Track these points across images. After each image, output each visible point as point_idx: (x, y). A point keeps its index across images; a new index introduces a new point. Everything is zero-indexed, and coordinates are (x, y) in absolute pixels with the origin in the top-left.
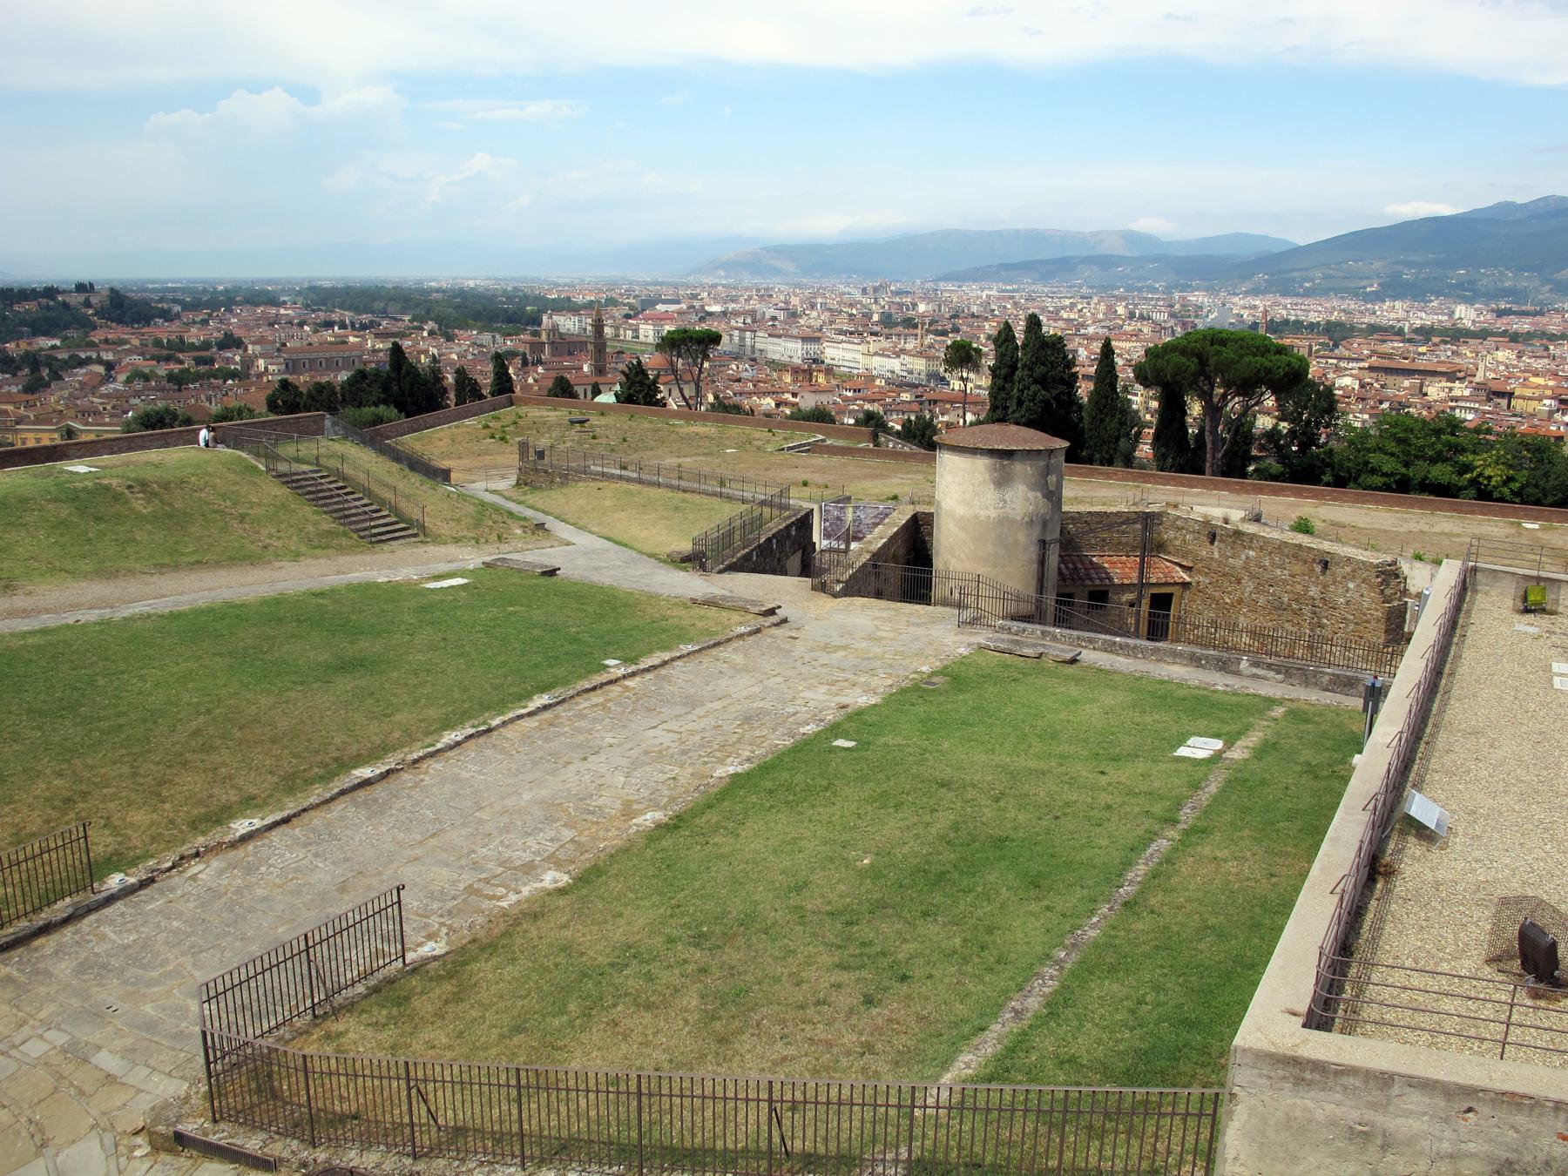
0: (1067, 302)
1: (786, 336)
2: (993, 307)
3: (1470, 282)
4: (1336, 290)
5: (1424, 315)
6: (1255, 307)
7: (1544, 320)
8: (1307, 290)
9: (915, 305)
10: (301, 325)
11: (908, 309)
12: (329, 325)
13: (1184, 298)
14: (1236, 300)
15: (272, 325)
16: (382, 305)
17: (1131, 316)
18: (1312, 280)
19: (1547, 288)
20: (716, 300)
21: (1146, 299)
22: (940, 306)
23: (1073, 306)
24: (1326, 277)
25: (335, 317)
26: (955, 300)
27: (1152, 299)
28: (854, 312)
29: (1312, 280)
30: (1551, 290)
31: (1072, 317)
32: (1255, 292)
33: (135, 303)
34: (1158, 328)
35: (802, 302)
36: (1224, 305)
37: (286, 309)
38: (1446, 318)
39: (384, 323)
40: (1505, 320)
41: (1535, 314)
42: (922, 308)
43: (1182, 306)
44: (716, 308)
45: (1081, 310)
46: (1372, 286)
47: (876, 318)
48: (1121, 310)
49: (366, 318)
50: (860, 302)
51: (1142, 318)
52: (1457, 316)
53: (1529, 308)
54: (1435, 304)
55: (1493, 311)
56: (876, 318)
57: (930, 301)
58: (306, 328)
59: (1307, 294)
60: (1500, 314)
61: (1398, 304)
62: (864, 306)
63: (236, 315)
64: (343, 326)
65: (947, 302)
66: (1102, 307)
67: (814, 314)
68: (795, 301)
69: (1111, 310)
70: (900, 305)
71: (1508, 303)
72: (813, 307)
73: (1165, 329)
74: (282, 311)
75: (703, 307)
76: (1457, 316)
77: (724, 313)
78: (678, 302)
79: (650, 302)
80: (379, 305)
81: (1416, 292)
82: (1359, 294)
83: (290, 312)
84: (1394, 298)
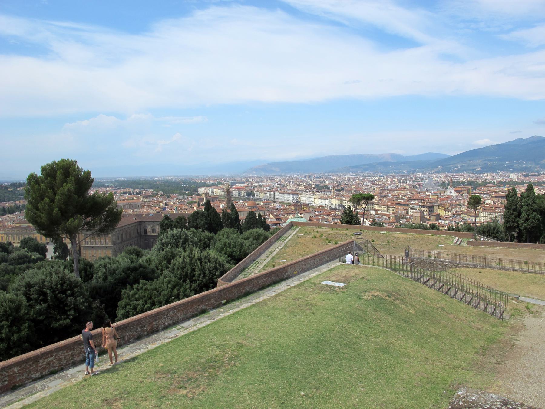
0: (377, 178)
2: (352, 181)
3: (511, 166)
4: (466, 170)
5: (499, 178)
6: (440, 177)
7: (541, 177)
8: (456, 170)
9: (324, 181)
12: (125, 193)
13: (415, 175)
14: (433, 175)
16: (142, 186)
17: (400, 182)
18: (457, 167)
19: (538, 166)
21: (402, 176)
22: (333, 181)
23: (379, 179)
24: (462, 166)
25: (127, 190)
26: (338, 179)
27: (404, 176)
28: (305, 184)
29: (457, 167)
30: (539, 167)
31: (380, 183)
32: (438, 172)
34: (411, 186)
35: (285, 181)
36: (429, 177)
37: (109, 188)
38: (507, 178)
39: (144, 192)
40: (527, 178)
41: (537, 176)
42: (327, 182)
43: (416, 178)
44: (257, 184)
45: (382, 181)
46: (478, 168)
47: (313, 186)
48: (396, 180)
49: (137, 191)
50: (306, 181)
51: (403, 182)
52: (511, 177)
53: (533, 173)
54: (501, 173)
55: (523, 175)
56: (313, 186)
57: (329, 180)
58: (117, 194)
59: (456, 172)
60: (525, 176)
61: (489, 174)
62: (307, 182)
64: (130, 193)
65: (335, 180)
66: (389, 179)
67: (291, 185)
68: (283, 181)
69: (392, 181)
70: (320, 181)
71: (525, 172)
72: (290, 182)
73: (413, 186)
74: (108, 189)
75: (252, 184)
76: (511, 177)
77: (261, 186)
78: (244, 183)
79: (234, 183)
81: (493, 170)
82: (473, 171)
83: (110, 189)
84: (487, 172)
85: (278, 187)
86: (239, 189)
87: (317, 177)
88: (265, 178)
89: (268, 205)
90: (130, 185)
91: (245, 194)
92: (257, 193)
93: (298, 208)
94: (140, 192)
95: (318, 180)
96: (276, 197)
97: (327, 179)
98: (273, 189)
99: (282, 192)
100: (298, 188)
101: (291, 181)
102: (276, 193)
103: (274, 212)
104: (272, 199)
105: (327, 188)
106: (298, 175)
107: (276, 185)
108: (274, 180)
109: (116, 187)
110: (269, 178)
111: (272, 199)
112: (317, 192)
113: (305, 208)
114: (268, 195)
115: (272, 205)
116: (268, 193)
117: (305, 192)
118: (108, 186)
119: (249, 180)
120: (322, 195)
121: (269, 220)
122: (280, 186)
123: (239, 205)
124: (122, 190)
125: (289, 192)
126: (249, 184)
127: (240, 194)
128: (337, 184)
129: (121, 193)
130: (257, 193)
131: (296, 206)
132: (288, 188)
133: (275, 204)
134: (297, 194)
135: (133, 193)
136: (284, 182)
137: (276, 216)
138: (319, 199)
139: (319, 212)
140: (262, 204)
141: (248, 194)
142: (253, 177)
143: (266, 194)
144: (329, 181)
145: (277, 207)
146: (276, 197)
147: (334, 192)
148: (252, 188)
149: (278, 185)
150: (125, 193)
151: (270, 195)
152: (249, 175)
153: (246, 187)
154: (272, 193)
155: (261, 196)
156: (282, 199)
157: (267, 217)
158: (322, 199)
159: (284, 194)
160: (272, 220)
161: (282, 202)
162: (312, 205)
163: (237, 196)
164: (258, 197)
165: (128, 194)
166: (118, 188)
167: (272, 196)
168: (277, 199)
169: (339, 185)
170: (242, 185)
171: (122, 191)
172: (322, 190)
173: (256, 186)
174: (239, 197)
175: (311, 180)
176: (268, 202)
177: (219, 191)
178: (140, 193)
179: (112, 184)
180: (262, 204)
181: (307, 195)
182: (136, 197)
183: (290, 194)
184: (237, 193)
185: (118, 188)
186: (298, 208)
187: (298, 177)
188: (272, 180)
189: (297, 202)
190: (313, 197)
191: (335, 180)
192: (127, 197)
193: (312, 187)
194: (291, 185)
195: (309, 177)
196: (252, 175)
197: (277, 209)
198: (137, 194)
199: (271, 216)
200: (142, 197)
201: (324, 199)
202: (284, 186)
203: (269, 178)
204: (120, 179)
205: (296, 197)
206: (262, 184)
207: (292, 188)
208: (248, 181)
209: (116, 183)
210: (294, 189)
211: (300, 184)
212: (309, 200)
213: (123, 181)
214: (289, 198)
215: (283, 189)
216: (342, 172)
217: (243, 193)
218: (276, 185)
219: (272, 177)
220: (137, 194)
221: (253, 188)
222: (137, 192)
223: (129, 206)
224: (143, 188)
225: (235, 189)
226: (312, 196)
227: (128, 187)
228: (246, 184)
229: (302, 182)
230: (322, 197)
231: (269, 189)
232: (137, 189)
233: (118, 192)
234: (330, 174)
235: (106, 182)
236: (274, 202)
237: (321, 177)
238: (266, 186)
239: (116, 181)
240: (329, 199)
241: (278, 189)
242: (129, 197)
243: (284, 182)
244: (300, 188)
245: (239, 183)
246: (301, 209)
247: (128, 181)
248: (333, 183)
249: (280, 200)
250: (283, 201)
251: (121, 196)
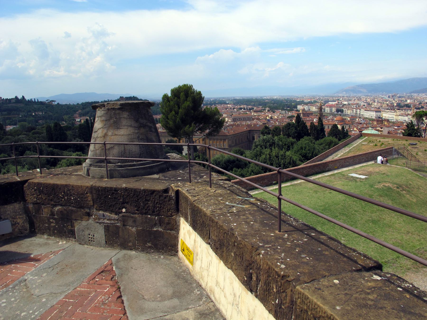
1: (370, 110)
9: (406, 101)
10: (234, 109)
11: (404, 102)
12: (241, 109)
15: (226, 109)
16: (253, 103)
20: (345, 100)
22: (414, 101)
25: (242, 106)
26: (419, 98)
28: (388, 103)
35: (371, 101)
37: (229, 105)
47: (395, 105)
49: (250, 107)
50: (389, 100)
56: (395, 105)
57: (411, 99)
62: (390, 101)
64: (244, 109)
67: (376, 104)
70: (402, 101)
72: (374, 102)
74: (228, 105)
75: (342, 102)
77: (349, 104)
78: (335, 101)
79: (327, 102)
80: (253, 103)
83: (230, 106)
85: (364, 105)
86: (331, 106)
87: (399, 97)
88: (353, 97)
89: (354, 120)
91: (335, 110)
92: (345, 110)
93: (379, 123)
95: (400, 99)
96: (361, 113)
97: (408, 99)
98: (359, 106)
99: (366, 109)
100: (382, 106)
101: (376, 100)
102: (361, 110)
103: (358, 126)
104: (358, 115)
105: (408, 106)
106: (383, 95)
107: (362, 104)
108: (361, 99)
109: (234, 104)
110: (357, 97)
111: (358, 115)
112: (398, 109)
113: (386, 123)
114: (355, 112)
115: (357, 120)
116: (355, 110)
117: (387, 109)
118: (228, 104)
119: (339, 99)
120: (402, 112)
121: (353, 132)
122: (366, 104)
123: (329, 119)
124: (238, 106)
125: (373, 109)
126: (339, 103)
127: (331, 110)
128: (418, 103)
129: (238, 109)
130: (345, 110)
131: (378, 121)
132: (373, 106)
133: (360, 120)
134: (380, 111)
135: (247, 109)
136: (369, 101)
137: (359, 129)
138: (400, 115)
139: (398, 127)
140: (349, 119)
141: (338, 111)
142: (343, 97)
143: (353, 111)
144: (410, 100)
145: (361, 122)
146: (361, 113)
147: (414, 110)
148: (341, 106)
149: (364, 104)
150: (241, 109)
151: (356, 111)
152: (340, 95)
153: (337, 104)
154: (358, 110)
155: (349, 112)
156: (366, 115)
157: (352, 129)
158: (402, 116)
159: (368, 111)
160: (356, 132)
161: (366, 118)
162: (393, 121)
163: (329, 112)
164: (346, 113)
167: (358, 112)
168: (362, 115)
169: (419, 104)
170: (334, 103)
172: (403, 108)
173: (345, 105)
174: (330, 113)
175: (394, 100)
176: (353, 118)
177: (314, 108)
178: (252, 109)
179: (232, 102)
180: (349, 119)
181: (388, 112)
183: (374, 111)
184: (329, 110)
186: (379, 123)
187: (383, 97)
188: (359, 99)
189: (379, 118)
190: (394, 114)
191: (416, 99)
193: (394, 105)
194: (376, 104)
195: (393, 96)
196: (343, 95)
197: (361, 124)
198: (250, 109)
199: (355, 129)
201: (404, 116)
202: (369, 104)
203: (357, 97)
204: (238, 98)
205: (378, 114)
206: (350, 102)
207: (376, 106)
208: (338, 100)
209: (235, 101)
210: (378, 107)
211: (384, 103)
212: (390, 116)
213: (240, 99)
214: (372, 115)
215: (368, 106)
216: (423, 93)
217: (334, 110)
218: (362, 104)
219: (360, 97)
221: (342, 106)
224: (254, 105)
225: (327, 106)
226: (393, 113)
227: (243, 104)
228: (337, 102)
229: (386, 101)
230: (402, 114)
231: (356, 107)
234: (413, 94)
236: (360, 118)
237: (403, 97)
238: (353, 104)
239: (235, 100)
240: (408, 116)
241: (364, 107)
243: (369, 101)
244: (383, 106)
245: (331, 101)
246: (382, 124)
247: (244, 99)
248: (414, 102)
249: (365, 116)
250: (367, 117)
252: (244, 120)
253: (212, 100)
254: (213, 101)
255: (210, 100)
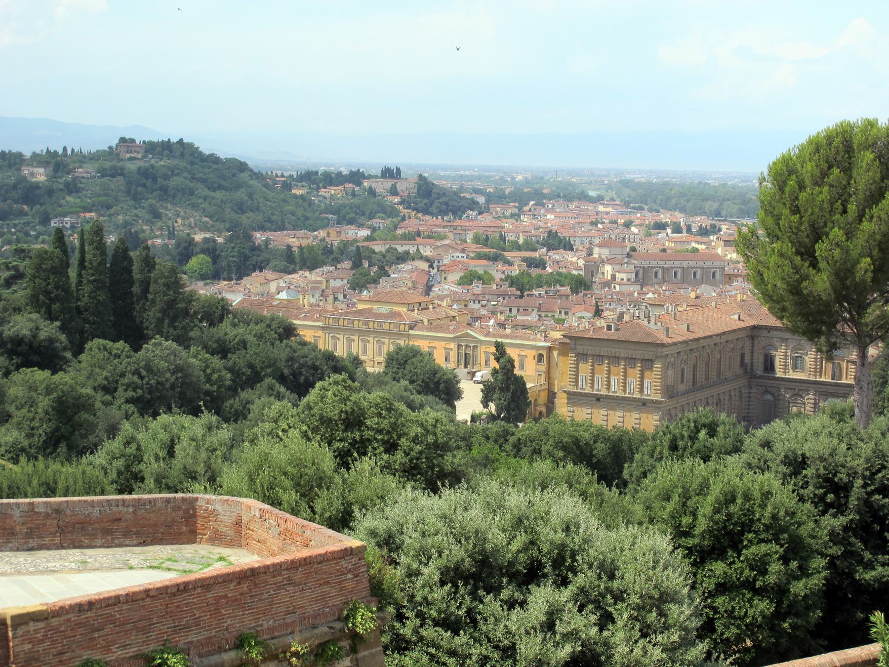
10: (628, 225)
12: (661, 226)
15: (594, 224)
16: (715, 205)
25: (665, 217)
33: (443, 193)
37: (606, 206)
39: (724, 227)
49: (700, 221)
58: (634, 230)
63: (549, 211)
64: (677, 229)
74: (601, 208)
83: (610, 209)
90: (674, 201)
94: (713, 226)
109: (627, 204)
118: (599, 199)
124: (647, 214)
129: (648, 227)
150: (661, 226)
165: (669, 231)
166: (634, 208)
171: (650, 218)
178: (715, 230)
182: (701, 243)
185: (634, 208)
192: (667, 239)
198: (704, 232)
200: (722, 243)
204: (639, 178)
209: (627, 192)
213: (650, 184)
220: (704, 232)
222: (701, 227)
223: (663, 272)
224: (718, 214)
227: (666, 205)
232: (701, 214)
233: (637, 222)
235: (590, 183)
239: (627, 183)
242: (676, 242)
247: (666, 184)
251: (649, 235)
252: (683, 281)
253: (519, 178)
254: (527, 182)
255: (513, 178)
